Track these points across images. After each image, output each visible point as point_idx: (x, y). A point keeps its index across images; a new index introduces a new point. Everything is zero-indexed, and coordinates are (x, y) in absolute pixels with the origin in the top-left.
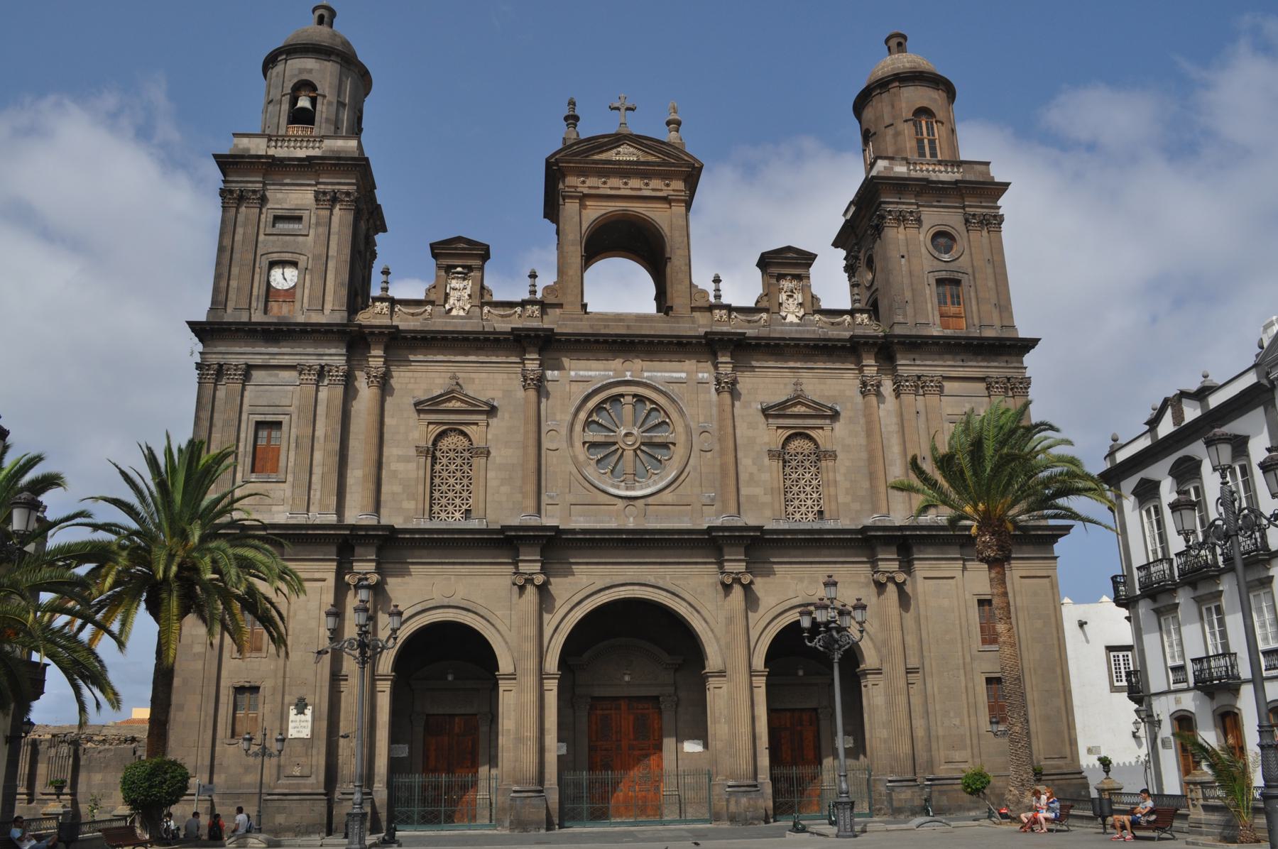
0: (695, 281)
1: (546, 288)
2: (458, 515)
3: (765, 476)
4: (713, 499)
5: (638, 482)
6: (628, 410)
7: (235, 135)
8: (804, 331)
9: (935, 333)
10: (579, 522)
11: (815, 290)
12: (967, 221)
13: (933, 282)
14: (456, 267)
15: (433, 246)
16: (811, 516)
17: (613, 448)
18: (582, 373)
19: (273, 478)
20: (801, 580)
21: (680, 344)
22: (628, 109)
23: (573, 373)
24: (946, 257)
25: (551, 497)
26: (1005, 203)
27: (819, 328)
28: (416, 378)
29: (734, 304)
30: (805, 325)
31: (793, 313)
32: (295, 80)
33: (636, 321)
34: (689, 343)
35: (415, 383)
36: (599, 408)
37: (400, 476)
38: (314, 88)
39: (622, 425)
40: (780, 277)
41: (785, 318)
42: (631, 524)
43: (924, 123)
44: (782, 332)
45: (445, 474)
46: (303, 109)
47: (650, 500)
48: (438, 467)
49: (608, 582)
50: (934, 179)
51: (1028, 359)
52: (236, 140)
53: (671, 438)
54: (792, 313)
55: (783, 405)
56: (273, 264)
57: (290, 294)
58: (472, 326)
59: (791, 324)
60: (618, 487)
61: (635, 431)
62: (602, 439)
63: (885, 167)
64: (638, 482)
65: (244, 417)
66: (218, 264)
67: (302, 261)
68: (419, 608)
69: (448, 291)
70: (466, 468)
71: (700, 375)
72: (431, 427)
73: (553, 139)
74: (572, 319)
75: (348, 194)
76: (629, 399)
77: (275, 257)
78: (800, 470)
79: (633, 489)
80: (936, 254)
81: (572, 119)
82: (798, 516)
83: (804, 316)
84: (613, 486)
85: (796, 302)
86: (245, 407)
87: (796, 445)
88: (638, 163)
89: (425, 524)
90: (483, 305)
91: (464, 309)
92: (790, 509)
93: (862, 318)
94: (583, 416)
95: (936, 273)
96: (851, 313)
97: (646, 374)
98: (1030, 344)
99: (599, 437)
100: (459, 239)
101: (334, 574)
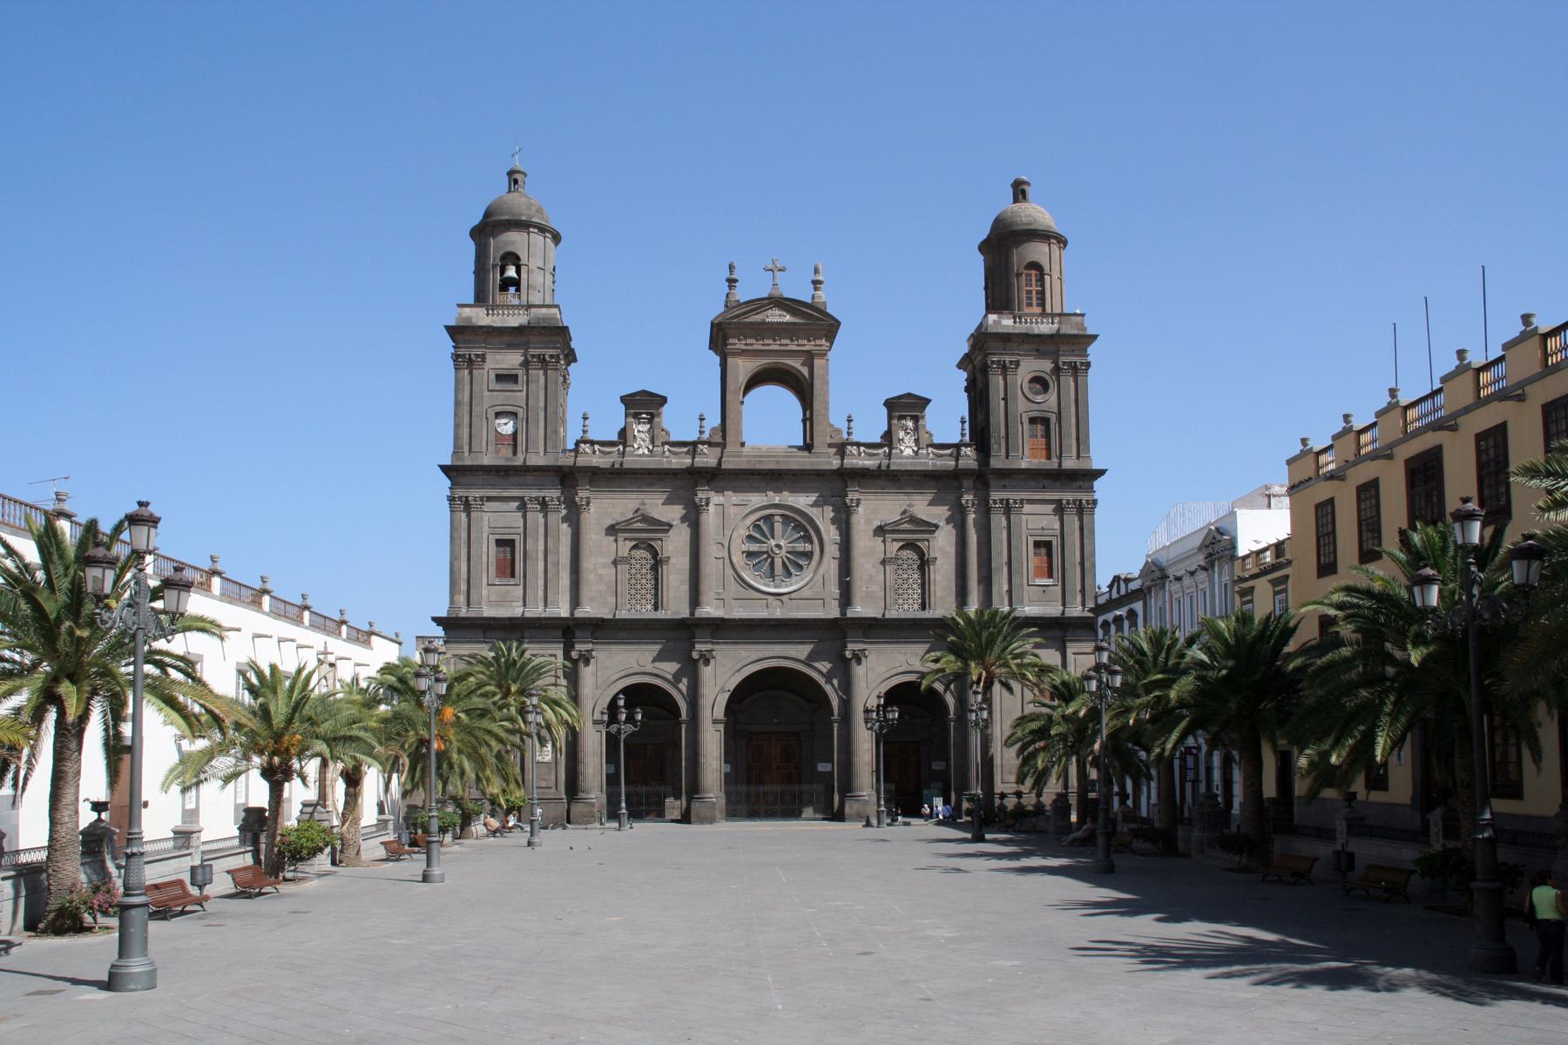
1: (713, 429)
2: (649, 607)
5: (784, 581)
6: (778, 527)
7: (460, 306)
9: (1024, 465)
10: (740, 612)
11: (928, 428)
12: (1057, 370)
13: (1026, 421)
14: (641, 413)
16: (916, 606)
17: (766, 556)
19: (512, 581)
20: (905, 654)
22: (780, 270)
24: (1039, 399)
25: (718, 593)
26: (1093, 351)
27: (930, 461)
28: (613, 504)
30: (919, 458)
31: (911, 447)
32: (502, 252)
33: (784, 456)
34: (823, 475)
35: (613, 508)
36: (757, 527)
38: (520, 260)
39: (773, 537)
40: (901, 418)
41: (902, 452)
42: (778, 613)
43: (1033, 275)
44: (899, 464)
45: (639, 576)
47: (793, 596)
48: (633, 571)
49: (761, 655)
50: (1036, 331)
51: (1097, 484)
52: (460, 310)
53: (808, 547)
54: (907, 448)
55: (896, 523)
56: (498, 415)
58: (652, 463)
59: (909, 457)
60: (768, 586)
61: (782, 544)
63: (994, 321)
64: (784, 581)
66: (456, 415)
67: (521, 413)
68: (623, 674)
69: (636, 433)
72: (626, 542)
73: (716, 309)
74: (734, 456)
75: (551, 356)
76: (777, 518)
77: (499, 409)
78: (910, 572)
79: (780, 587)
80: (1031, 396)
81: (732, 282)
82: (906, 606)
84: (765, 585)
85: (913, 438)
87: (909, 554)
88: (786, 323)
89: (623, 614)
90: (663, 444)
91: (648, 449)
92: (901, 601)
93: (968, 451)
94: (743, 532)
95: (1029, 413)
96: (957, 446)
97: (790, 499)
98: (1101, 472)
99: (754, 547)
101: (562, 652)
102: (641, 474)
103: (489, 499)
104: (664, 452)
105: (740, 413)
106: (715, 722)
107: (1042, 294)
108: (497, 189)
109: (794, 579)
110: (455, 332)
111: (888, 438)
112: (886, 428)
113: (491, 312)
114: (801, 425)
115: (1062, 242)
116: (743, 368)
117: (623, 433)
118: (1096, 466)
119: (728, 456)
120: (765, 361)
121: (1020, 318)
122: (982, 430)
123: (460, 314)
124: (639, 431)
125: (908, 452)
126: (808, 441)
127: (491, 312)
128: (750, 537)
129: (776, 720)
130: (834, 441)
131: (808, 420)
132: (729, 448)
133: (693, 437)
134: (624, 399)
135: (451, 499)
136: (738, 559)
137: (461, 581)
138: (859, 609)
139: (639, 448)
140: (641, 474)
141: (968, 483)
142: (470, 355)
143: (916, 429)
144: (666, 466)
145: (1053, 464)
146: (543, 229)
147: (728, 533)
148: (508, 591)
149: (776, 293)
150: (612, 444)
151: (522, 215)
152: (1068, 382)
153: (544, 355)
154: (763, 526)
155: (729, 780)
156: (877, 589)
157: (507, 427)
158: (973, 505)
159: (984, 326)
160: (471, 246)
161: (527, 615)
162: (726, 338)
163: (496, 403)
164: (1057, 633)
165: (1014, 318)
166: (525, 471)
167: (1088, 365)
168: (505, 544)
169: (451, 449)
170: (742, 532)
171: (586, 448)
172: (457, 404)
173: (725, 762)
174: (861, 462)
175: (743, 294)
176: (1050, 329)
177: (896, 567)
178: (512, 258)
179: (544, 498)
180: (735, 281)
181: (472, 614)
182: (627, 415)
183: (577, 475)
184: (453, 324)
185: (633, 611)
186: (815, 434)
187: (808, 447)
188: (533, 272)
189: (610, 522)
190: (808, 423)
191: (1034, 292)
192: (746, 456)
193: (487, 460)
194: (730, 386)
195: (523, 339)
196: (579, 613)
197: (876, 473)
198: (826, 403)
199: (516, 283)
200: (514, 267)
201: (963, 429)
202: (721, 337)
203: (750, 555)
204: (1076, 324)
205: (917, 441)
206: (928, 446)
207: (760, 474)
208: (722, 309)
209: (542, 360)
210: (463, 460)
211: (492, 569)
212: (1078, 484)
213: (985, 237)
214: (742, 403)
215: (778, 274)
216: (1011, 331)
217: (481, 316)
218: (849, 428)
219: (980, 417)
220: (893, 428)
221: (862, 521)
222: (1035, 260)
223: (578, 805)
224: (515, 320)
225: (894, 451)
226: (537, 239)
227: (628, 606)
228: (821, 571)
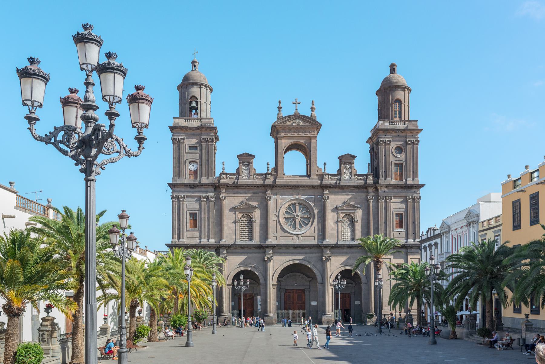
0: (318, 165)
3: (336, 228)
4: (321, 235)
6: (297, 208)
8: (351, 182)
10: (283, 241)
11: (355, 168)
12: (406, 143)
14: (245, 162)
15: (237, 156)
18: (283, 196)
21: (312, 187)
23: (281, 196)
24: (398, 155)
25: (274, 234)
26: (421, 136)
27: (355, 181)
29: (330, 173)
37: (231, 228)
38: (197, 99)
39: (295, 212)
42: (297, 242)
44: (344, 182)
46: (193, 107)
47: (303, 235)
50: (398, 128)
51: (421, 190)
57: (196, 172)
59: (347, 180)
60: (294, 231)
61: (299, 215)
62: (289, 217)
65: (185, 212)
70: (250, 226)
71: (319, 196)
74: (281, 179)
77: (190, 160)
79: (298, 232)
81: (280, 108)
83: (351, 176)
84: (292, 231)
86: (186, 209)
89: (238, 242)
92: (344, 237)
93: (370, 177)
96: (366, 175)
99: (288, 216)
100: (246, 153)
102: (245, 186)
103: (187, 197)
104: (254, 178)
105: (283, 162)
106: (273, 285)
107: (400, 112)
108: (188, 69)
109: (303, 228)
110: (172, 129)
111: (340, 172)
112: (339, 168)
113: (186, 121)
114: (306, 167)
115: (409, 90)
116: (284, 143)
117: (238, 170)
118: (421, 183)
119: (278, 180)
120: (292, 141)
121: (392, 122)
122: (376, 168)
123: (174, 122)
124: (244, 169)
125: (347, 177)
126: (309, 173)
127: (186, 121)
128: (287, 212)
129: (296, 284)
130: (319, 173)
131: (309, 165)
132: (279, 176)
133: (265, 171)
134: (238, 157)
135: (172, 197)
136: (282, 221)
137: (177, 231)
138: (328, 240)
139: (244, 176)
140: (245, 186)
141: (371, 190)
142: (178, 138)
143: (351, 168)
144: (255, 184)
145: (403, 182)
146: (206, 86)
147: (278, 210)
148: (194, 233)
149: (297, 113)
150: (234, 175)
151: (198, 80)
152: (410, 147)
153: (207, 139)
154: (291, 208)
155: (279, 308)
156: (335, 233)
157: (192, 168)
158: (372, 198)
159: (378, 126)
160: (177, 94)
161: (202, 243)
162: (277, 132)
163: (189, 158)
164: (404, 250)
165: (390, 122)
166: (201, 185)
167: (418, 141)
168: (193, 215)
169: (172, 177)
170: (283, 210)
171: (224, 176)
172: (174, 158)
173: (277, 301)
174: (329, 182)
175: (285, 113)
176: (404, 127)
177: (342, 224)
178: (194, 98)
179: (208, 196)
180: (281, 108)
181: (181, 243)
182: (239, 163)
183: (221, 187)
184: (172, 126)
185: (242, 241)
186: (312, 170)
187: (309, 176)
188: (202, 104)
189: (233, 206)
190: (309, 166)
191: (398, 111)
192: (285, 179)
193: (186, 181)
194: (279, 151)
195: (198, 132)
196: (221, 242)
197: (335, 186)
198: (316, 158)
199: (196, 109)
200: (195, 102)
201: (369, 168)
202: (275, 131)
203: (286, 219)
204: (414, 124)
205: (351, 173)
206: (355, 175)
207: (290, 187)
208: (276, 120)
209: (207, 140)
210: (177, 181)
211: (188, 225)
212: (413, 190)
213: (378, 89)
214: (284, 158)
215: (298, 105)
216: (388, 128)
217: (183, 122)
218: (325, 168)
219: (375, 163)
220: (342, 168)
221: (329, 205)
222: (398, 98)
223: (221, 318)
224: (196, 124)
225: (342, 177)
226: (204, 90)
227: (240, 239)
228: (313, 226)
